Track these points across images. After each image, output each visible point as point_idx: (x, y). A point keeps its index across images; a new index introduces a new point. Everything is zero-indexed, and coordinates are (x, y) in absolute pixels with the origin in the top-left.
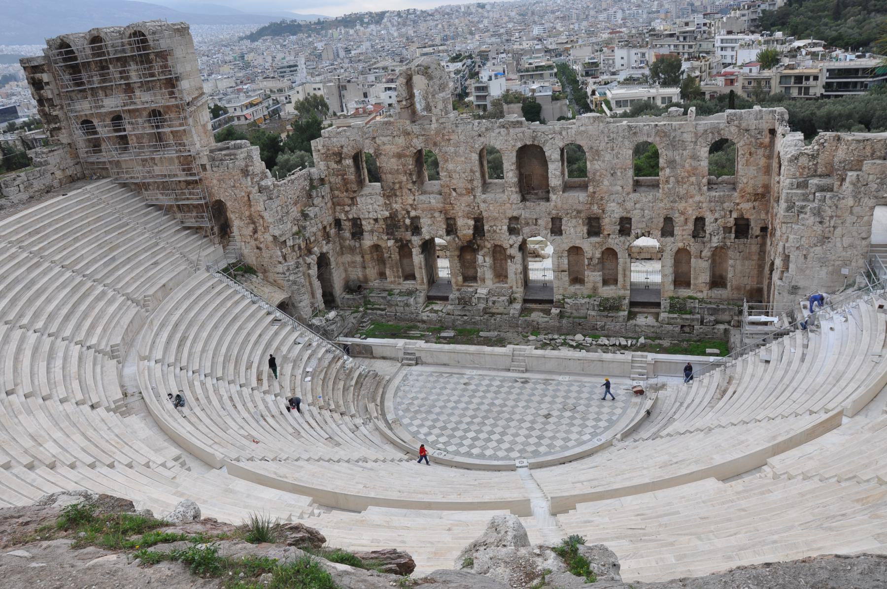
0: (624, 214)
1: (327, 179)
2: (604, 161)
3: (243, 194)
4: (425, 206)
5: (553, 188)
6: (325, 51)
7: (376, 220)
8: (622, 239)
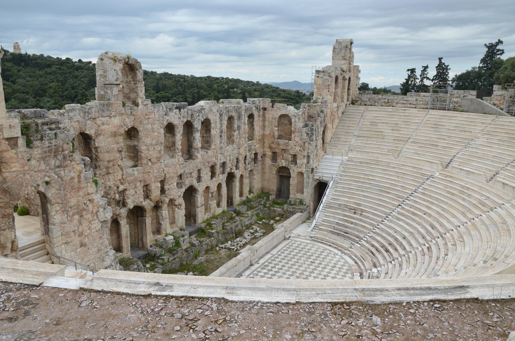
0: (225, 160)
3: (72, 174)
4: (131, 178)
8: (224, 175)
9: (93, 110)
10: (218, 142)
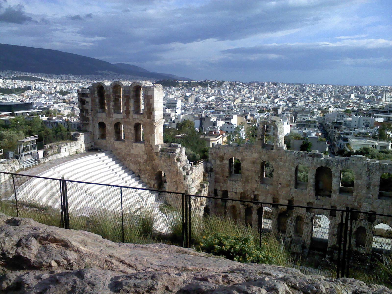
1: (214, 169)
2: (364, 180)
3: (174, 170)
5: (334, 190)
6: (190, 98)
7: (236, 193)
9: (241, 148)
10: (364, 192)
